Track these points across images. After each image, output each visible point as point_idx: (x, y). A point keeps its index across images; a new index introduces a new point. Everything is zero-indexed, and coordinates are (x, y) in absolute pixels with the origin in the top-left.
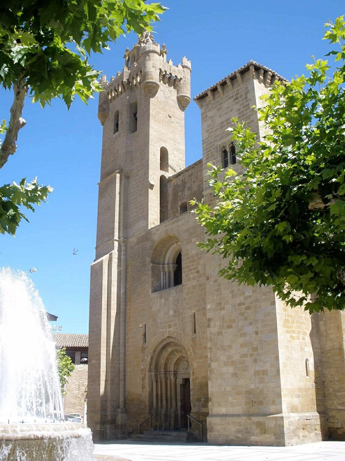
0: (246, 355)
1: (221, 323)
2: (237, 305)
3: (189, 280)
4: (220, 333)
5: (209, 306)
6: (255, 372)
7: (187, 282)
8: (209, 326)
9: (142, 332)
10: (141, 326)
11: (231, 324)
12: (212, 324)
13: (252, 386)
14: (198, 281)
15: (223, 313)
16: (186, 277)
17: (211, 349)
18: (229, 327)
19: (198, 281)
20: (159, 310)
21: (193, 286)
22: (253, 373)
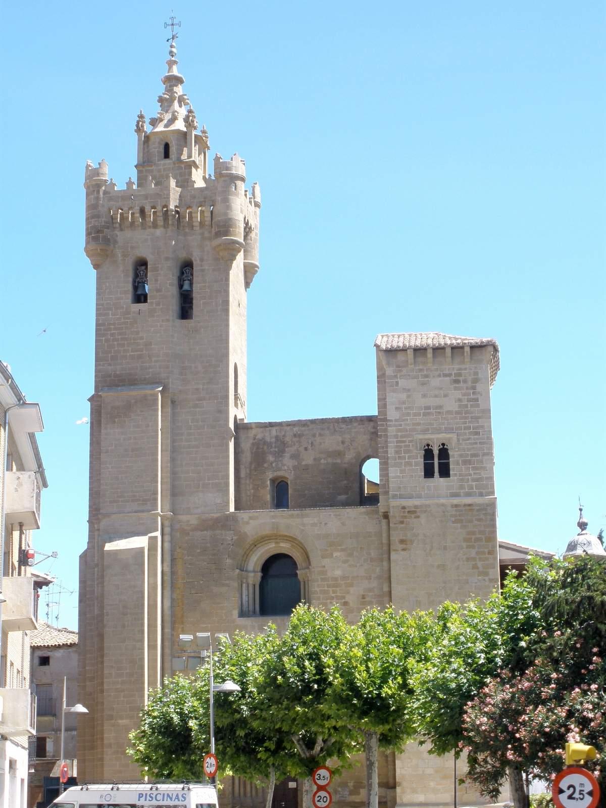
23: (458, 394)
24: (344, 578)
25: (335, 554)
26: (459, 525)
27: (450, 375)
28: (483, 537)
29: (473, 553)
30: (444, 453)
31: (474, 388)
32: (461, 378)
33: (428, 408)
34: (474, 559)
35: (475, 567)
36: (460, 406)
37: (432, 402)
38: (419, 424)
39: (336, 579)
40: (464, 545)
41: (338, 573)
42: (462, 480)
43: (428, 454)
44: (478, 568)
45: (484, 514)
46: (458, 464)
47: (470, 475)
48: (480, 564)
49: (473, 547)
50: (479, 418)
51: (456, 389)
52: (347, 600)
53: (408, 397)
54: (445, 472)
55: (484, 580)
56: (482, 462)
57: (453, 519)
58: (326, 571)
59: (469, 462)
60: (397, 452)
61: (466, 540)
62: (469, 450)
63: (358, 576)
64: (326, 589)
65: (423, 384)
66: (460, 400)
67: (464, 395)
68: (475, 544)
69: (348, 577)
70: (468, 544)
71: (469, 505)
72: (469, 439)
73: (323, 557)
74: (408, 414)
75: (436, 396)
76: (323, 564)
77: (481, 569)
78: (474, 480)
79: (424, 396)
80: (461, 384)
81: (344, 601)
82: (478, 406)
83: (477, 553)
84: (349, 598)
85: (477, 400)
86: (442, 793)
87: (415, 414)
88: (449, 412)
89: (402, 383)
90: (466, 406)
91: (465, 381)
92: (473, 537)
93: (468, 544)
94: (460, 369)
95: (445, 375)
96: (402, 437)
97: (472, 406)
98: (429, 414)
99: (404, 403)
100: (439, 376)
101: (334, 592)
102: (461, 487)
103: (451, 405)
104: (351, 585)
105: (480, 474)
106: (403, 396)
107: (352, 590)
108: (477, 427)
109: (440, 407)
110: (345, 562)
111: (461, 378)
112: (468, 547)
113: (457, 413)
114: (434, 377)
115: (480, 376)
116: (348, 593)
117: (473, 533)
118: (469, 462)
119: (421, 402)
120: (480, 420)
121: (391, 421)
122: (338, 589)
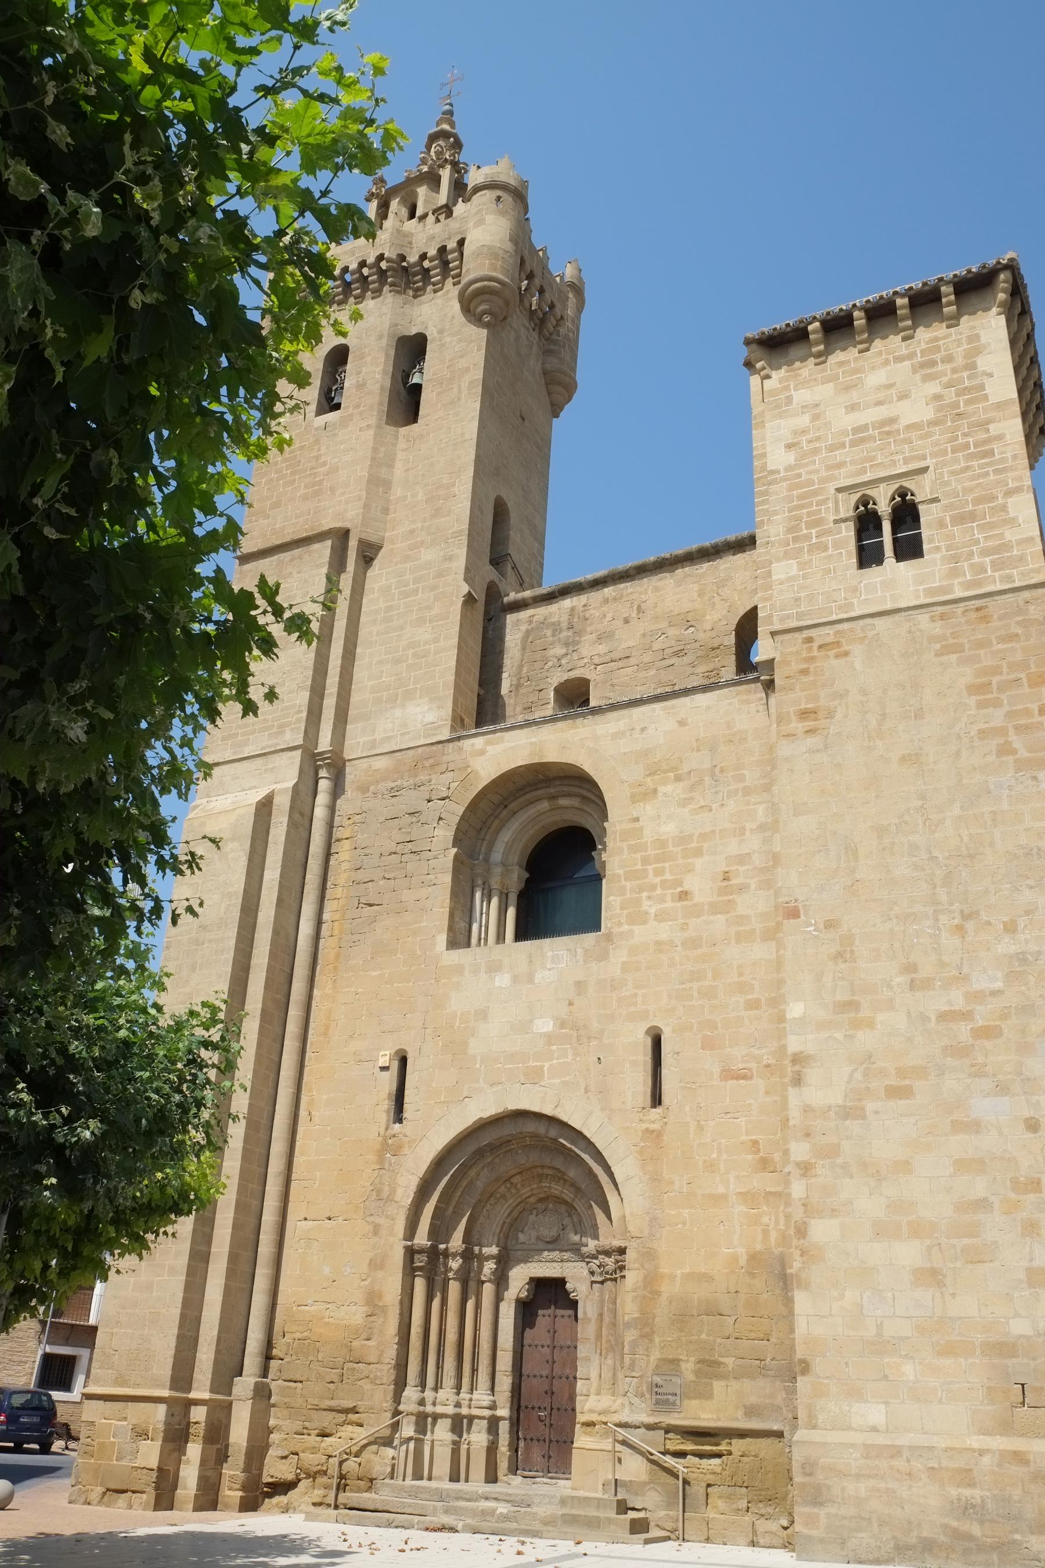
0: (982, 1204)
1: (858, 1075)
2: (933, 1018)
3: (639, 918)
4: (850, 1112)
5: (795, 1010)
6: (1029, 1271)
7: (626, 927)
8: (798, 1081)
9: (388, 1082)
10: (383, 1061)
11: (907, 1082)
12: (813, 1074)
13: (1020, 1327)
14: (684, 927)
15: (865, 1039)
16: (622, 909)
17: (806, 1169)
18: (895, 1092)
19: (684, 927)
20: (483, 1015)
21: (658, 943)
22: (1022, 1275)
23: (934, 388)
24: (682, 839)
25: (662, 789)
26: (954, 657)
27: (911, 356)
28: (1023, 675)
29: (997, 717)
30: (906, 513)
31: (972, 366)
32: (938, 357)
33: (864, 428)
34: (1002, 731)
35: (1005, 750)
36: (939, 409)
37: (869, 416)
38: (841, 465)
39: (662, 843)
40: (972, 701)
41: (669, 829)
42: (956, 559)
43: (867, 522)
44: (1014, 752)
45: (1018, 623)
46: (942, 524)
47: (978, 542)
48: (1017, 742)
49: (997, 704)
50: (989, 422)
51: (926, 378)
52: (686, 888)
53: (816, 417)
54: (909, 548)
55: (1035, 778)
56: (1004, 508)
57: (938, 646)
58: (641, 829)
59: (972, 517)
60: (790, 530)
61: (974, 689)
62: (967, 491)
63: (713, 831)
64: (639, 867)
65: (848, 388)
66: (937, 397)
67: (949, 385)
68: (1004, 697)
69: (691, 836)
70: (982, 697)
71: (978, 609)
72: (968, 468)
73: (634, 799)
74: (816, 451)
75: (879, 403)
76: (635, 815)
77: (1023, 753)
78: (985, 552)
79: (852, 408)
80: (940, 367)
81: (679, 889)
82: (986, 397)
83: (1010, 715)
84: (691, 883)
85: (982, 387)
86: (940, 1401)
87: (831, 448)
88: (910, 427)
89: (801, 396)
90: (956, 405)
91: (949, 359)
92: (995, 680)
93: (982, 697)
94: (936, 339)
95: (899, 359)
96: (800, 497)
97: (968, 402)
98: (863, 440)
99: (804, 432)
100: (887, 363)
101: (659, 872)
102: (954, 573)
103: (916, 410)
104: (698, 852)
105: (1001, 536)
106: (805, 420)
107: (699, 863)
108: (988, 441)
109: (893, 420)
110: (683, 803)
111: (938, 357)
112: (982, 705)
113: (932, 423)
114: (873, 368)
115: (984, 340)
116: (689, 870)
117: (996, 671)
118: (972, 517)
119: (844, 421)
120: (991, 427)
121: (777, 472)
122: (667, 865)
